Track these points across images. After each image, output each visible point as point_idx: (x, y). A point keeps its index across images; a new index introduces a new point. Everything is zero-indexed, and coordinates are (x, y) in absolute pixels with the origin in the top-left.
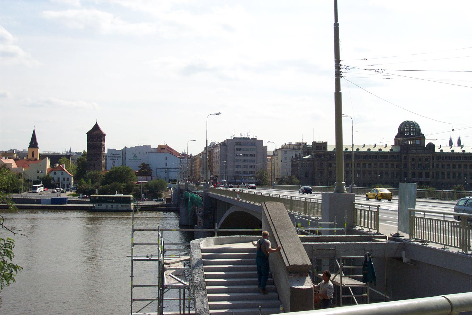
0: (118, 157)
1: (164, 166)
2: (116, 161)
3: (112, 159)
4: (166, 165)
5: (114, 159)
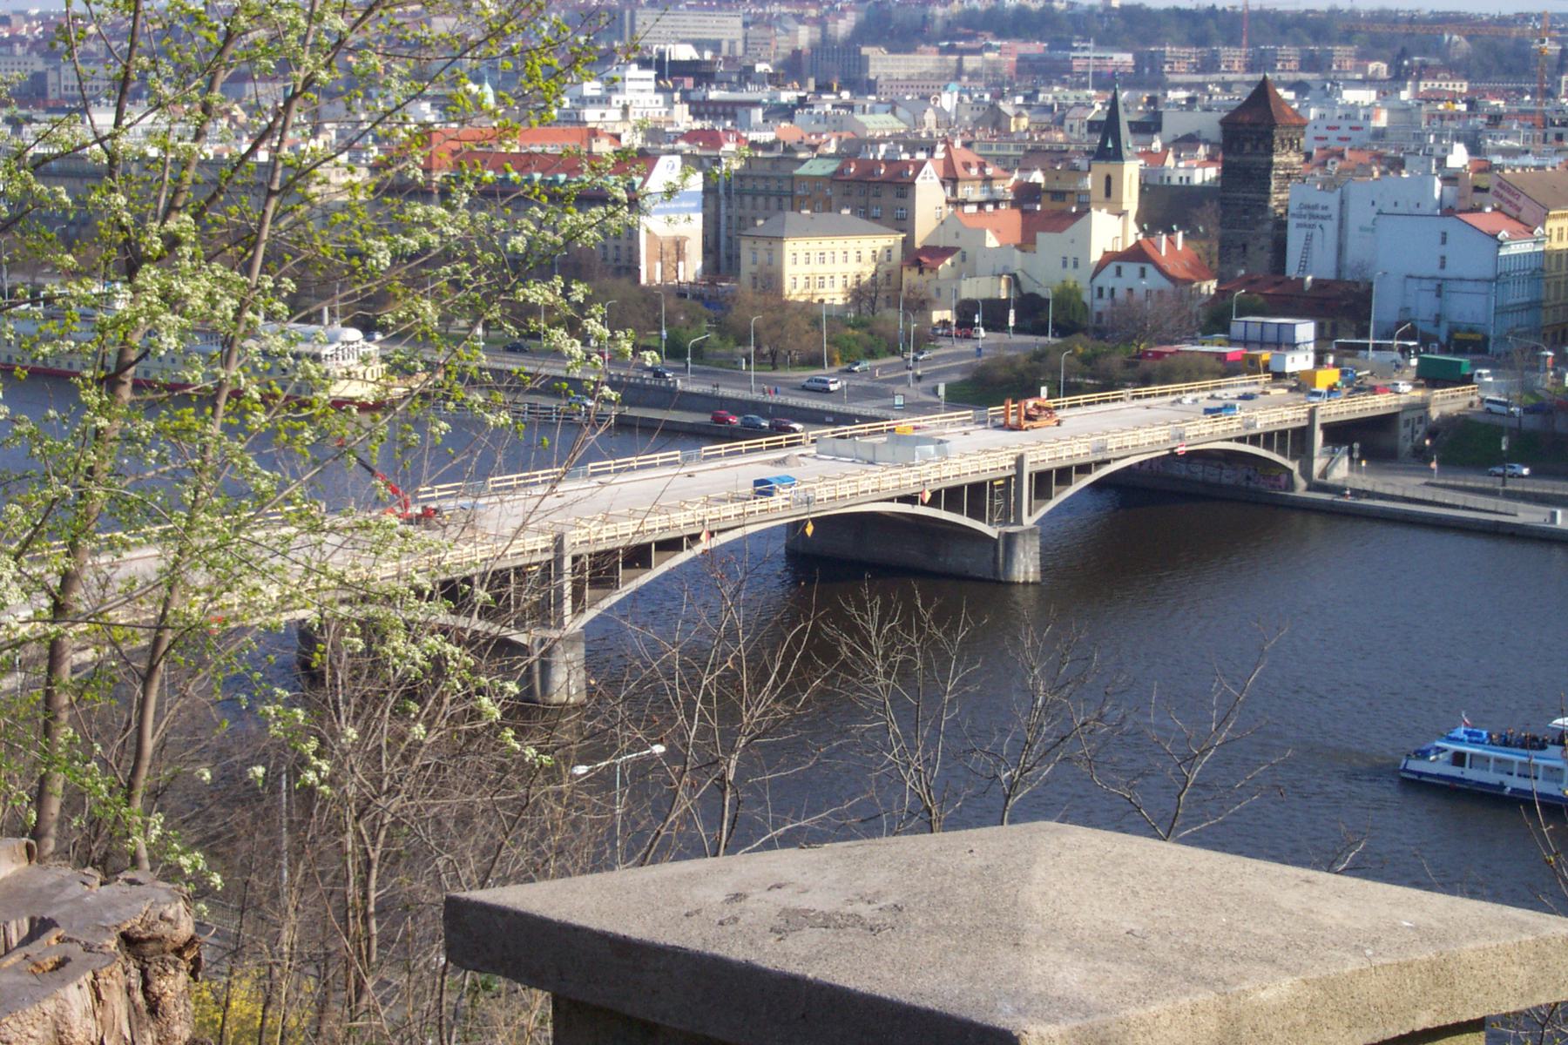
0: (1323, 218)
1: (1434, 270)
2: (1318, 230)
3: (1305, 226)
4: (1443, 266)
5: (1311, 226)
